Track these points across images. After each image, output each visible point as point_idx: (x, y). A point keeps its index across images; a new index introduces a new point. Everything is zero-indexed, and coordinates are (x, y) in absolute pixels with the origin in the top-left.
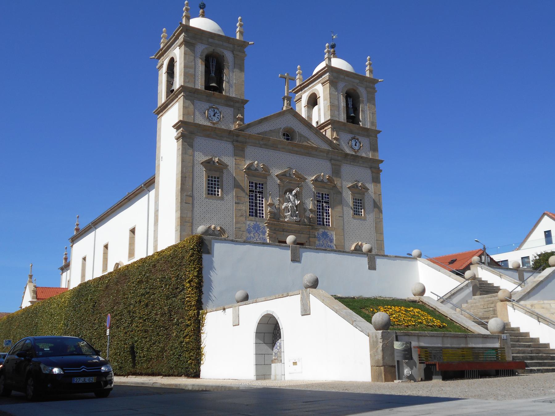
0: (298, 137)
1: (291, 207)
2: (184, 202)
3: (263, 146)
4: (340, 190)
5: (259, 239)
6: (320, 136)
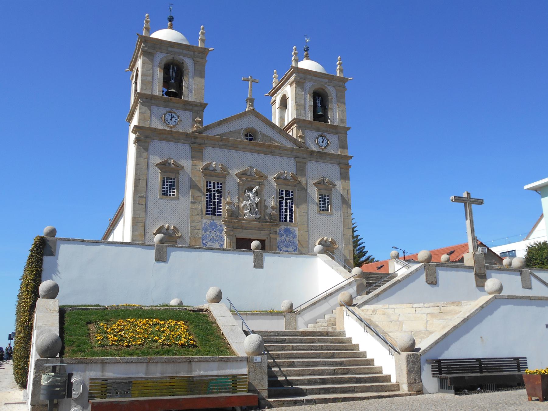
0: (260, 137)
1: (249, 204)
2: (138, 203)
3: (222, 147)
4: (305, 187)
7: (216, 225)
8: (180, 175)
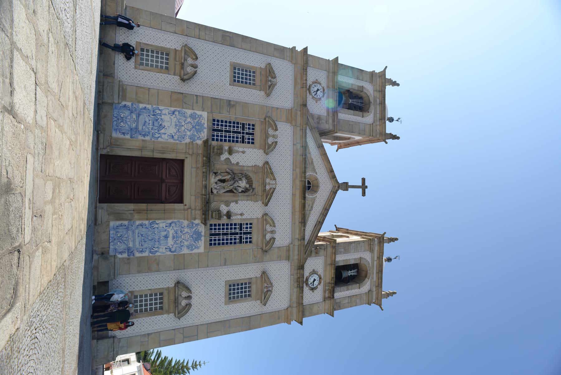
5: (184, 130)
7: (201, 132)
8: (259, 91)
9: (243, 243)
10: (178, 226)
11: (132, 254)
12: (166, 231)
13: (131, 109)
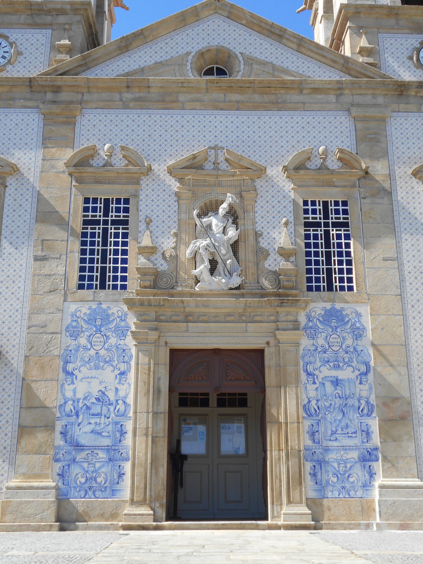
0: (242, 67)
3: (132, 104)
4: (386, 185)
5: (105, 350)
6: (312, 51)
7: (108, 315)
8: (7, 189)
9: (347, 219)
10: (312, 359)
11: (375, 452)
12: (324, 384)
13: (67, 463)
